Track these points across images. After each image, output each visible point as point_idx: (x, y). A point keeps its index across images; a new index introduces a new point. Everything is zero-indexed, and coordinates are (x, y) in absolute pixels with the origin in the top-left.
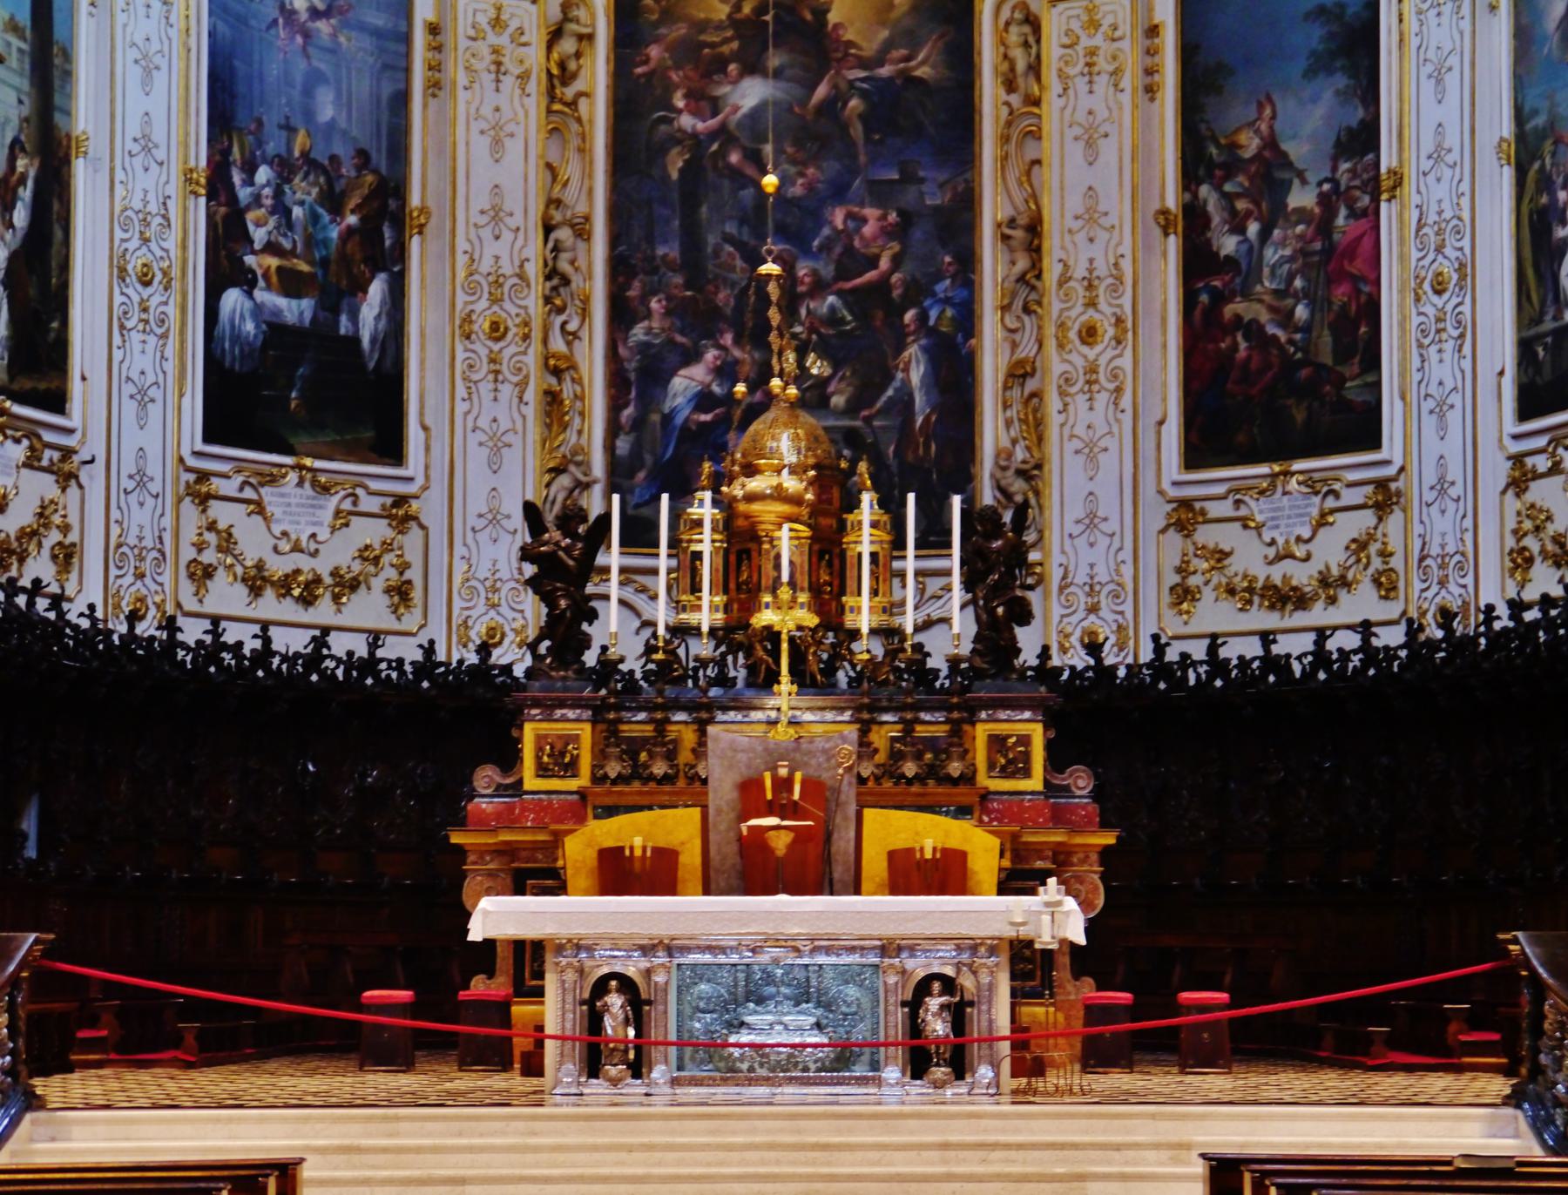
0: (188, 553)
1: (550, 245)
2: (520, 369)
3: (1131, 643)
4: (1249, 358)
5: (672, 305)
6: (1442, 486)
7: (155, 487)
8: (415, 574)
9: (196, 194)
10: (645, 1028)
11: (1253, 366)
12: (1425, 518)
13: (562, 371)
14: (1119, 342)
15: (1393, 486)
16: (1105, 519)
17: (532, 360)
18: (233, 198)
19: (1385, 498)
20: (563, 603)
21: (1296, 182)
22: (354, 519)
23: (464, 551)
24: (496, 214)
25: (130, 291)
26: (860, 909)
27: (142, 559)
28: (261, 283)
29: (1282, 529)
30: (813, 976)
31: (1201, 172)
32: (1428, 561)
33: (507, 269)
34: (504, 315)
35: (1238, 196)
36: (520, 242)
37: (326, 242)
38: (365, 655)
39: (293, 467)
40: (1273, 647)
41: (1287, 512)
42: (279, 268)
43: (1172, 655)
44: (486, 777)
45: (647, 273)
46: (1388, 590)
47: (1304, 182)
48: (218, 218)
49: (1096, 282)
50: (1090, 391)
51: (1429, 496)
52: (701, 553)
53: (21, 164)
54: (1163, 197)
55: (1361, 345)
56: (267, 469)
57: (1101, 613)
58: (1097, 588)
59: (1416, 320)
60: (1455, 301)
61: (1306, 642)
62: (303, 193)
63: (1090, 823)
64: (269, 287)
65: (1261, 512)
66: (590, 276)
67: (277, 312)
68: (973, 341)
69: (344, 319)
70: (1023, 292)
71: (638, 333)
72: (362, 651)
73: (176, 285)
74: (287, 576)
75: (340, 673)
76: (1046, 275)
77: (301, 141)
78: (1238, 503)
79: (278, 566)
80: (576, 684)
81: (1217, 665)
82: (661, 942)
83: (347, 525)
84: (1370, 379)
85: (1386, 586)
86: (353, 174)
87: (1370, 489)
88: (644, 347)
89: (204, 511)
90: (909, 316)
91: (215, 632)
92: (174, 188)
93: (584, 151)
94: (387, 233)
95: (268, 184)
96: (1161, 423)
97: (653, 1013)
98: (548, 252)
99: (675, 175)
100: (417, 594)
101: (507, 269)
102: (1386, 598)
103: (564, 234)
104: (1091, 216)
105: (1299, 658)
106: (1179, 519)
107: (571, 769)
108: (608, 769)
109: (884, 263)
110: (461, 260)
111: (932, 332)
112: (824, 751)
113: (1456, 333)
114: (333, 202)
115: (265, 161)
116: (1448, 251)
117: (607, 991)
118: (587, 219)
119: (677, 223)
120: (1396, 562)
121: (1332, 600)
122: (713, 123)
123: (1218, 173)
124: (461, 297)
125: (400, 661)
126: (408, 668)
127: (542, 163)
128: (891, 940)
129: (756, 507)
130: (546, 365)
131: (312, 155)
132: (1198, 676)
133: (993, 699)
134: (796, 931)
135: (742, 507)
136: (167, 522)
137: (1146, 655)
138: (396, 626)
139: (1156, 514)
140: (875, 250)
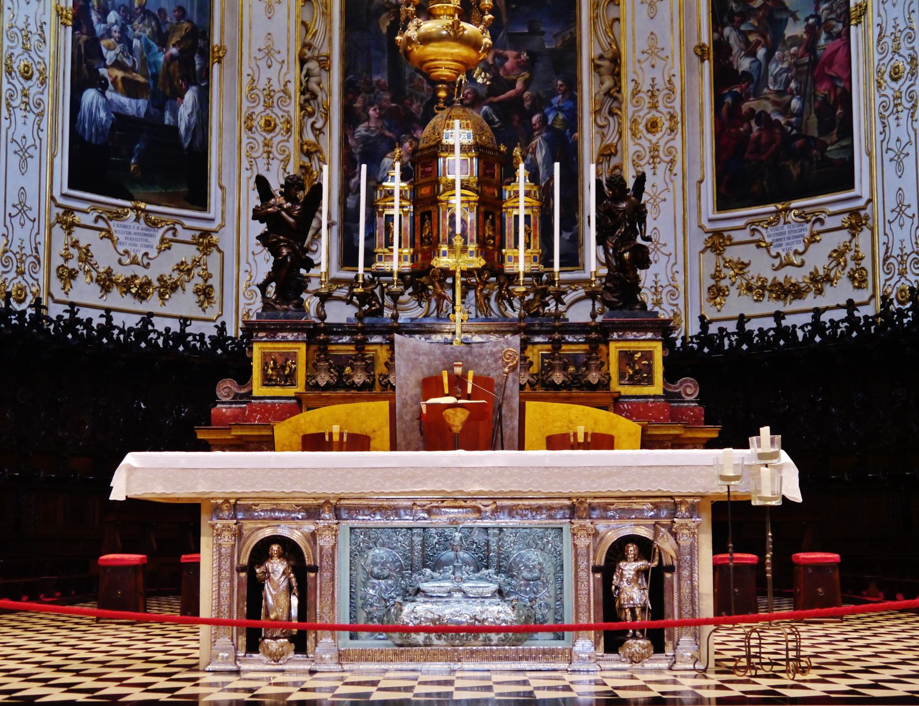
0: (57, 261)
1: (304, 72)
2: (284, 151)
3: (683, 324)
4: (759, 137)
5: (382, 113)
6: (900, 209)
7: (33, 214)
8: (214, 282)
9: (65, 25)
10: (310, 599)
11: (763, 141)
12: (888, 231)
13: (312, 153)
14: (672, 131)
15: (862, 213)
16: (665, 245)
17: (292, 146)
18: (91, 31)
19: (857, 221)
20: (285, 251)
21: (791, 20)
22: (173, 244)
23: (247, 267)
24: (269, 52)
25: (15, 82)
26: (547, 463)
27: (23, 262)
28: (111, 87)
29: (784, 246)
30: (493, 540)
31: (725, 19)
32: (891, 260)
33: (276, 86)
34: (274, 116)
35: (750, 32)
36: (284, 70)
37: (156, 64)
38: (178, 331)
39: (132, 209)
40: (783, 322)
41: (787, 235)
42: (123, 79)
43: (713, 329)
44: (226, 388)
45: (367, 92)
46: (860, 282)
47: (796, 19)
48: (81, 42)
49: (656, 93)
50: (654, 162)
51: (890, 216)
52: (393, 215)
54: (699, 38)
55: (838, 121)
56: (114, 209)
57: (663, 306)
58: (660, 289)
59: (879, 100)
60: (908, 83)
61: (808, 318)
62: (141, 32)
63: (697, 421)
64: (116, 90)
65: (769, 236)
66: (330, 93)
67: (122, 106)
68: (577, 134)
69: (167, 115)
70: (609, 102)
71: (361, 130)
72: (175, 327)
73: (50, 82)
74: (127, 279)
75: (160, 342)
76: (623, 90)
78: (754, 230)
79: (121, 273)
80: (297, 314)
81: (744, 335)
82: (327, 502)
83: (169, 248)
84: (844, 143)
85: (858, 279)
86: (175, 21)
87: (846, 216)
88: (365, 139)
89: (69, 234)
90: (535, 118)
91: (73, 313)
92: (51, 18)
93: (327, 14)
94: (197, 60)
95: (116, 21)
96: (701, 182)
97: (318, 580)
98: (303, 77)
99: (385, 30)
100: (216, 294)
101: (276, 86)
102: (859, 288)
103: (313, 65)
104: (653, 51)
105: (802, 328)
106: (713, 243)
107: (290, 379)
108: (319, 379)
109: (519, 85)
110: (246, 80)
111: (550, 129)
112: (492, 354)
113: (909, 105)
114: (162, 39)
115: (114, 8)
116: (901, 52)
117: (268, 557)
118: (328, 57)
119: (386, 60)
120: (866, 263)
121: (820, 292)
123: (737, 18)
124: (246, 104)
125: (202, 336)
126: (208, 341)
127: (299, 21)
128: (581, 499)
129: (431, 49)
130: (302, 149)
131: (146, 7)
132: (731, 341)
133: (622, 323)
134: (477, 488)
135: (418, 51)
136: (42, 238)
137: (694, 329)
138: (202, 315)
139: (698, 241)
140: (514, 77)
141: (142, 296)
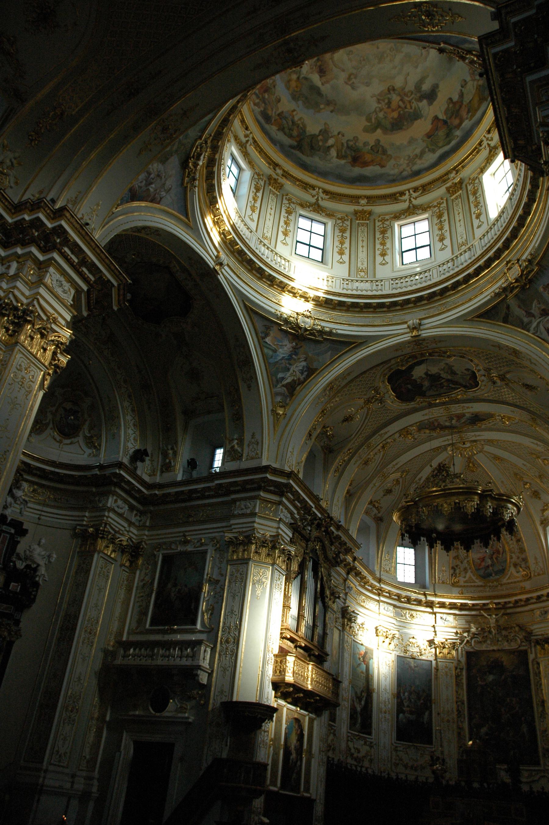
17: (455, 726)
53: (363, 694)
77: (413, 688)
79: (410, 764)
93: (462, 689)
122: (484, 683)
141: (416, 770)
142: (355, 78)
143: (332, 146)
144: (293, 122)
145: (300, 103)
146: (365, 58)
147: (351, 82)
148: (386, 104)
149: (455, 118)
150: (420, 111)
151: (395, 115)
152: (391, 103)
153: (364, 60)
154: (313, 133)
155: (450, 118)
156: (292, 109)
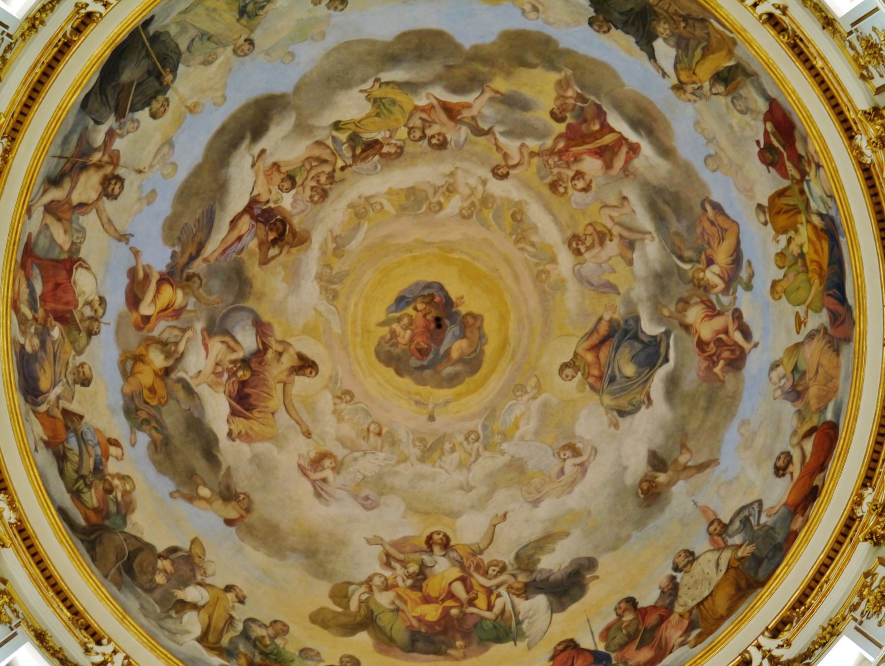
142: (337, 469)
143: (195, 607)
144: (98, 470)
145: (143, 439)
146: (384, 431)
147: (319, 475)
148: (409, 576)
149: (639, 648)
150: (519, 623)
151: (432, 613)
152: (425, 578)
153: (379, 434)
154: (148, 538)
155: (622, 647)
156: (114, 436)
